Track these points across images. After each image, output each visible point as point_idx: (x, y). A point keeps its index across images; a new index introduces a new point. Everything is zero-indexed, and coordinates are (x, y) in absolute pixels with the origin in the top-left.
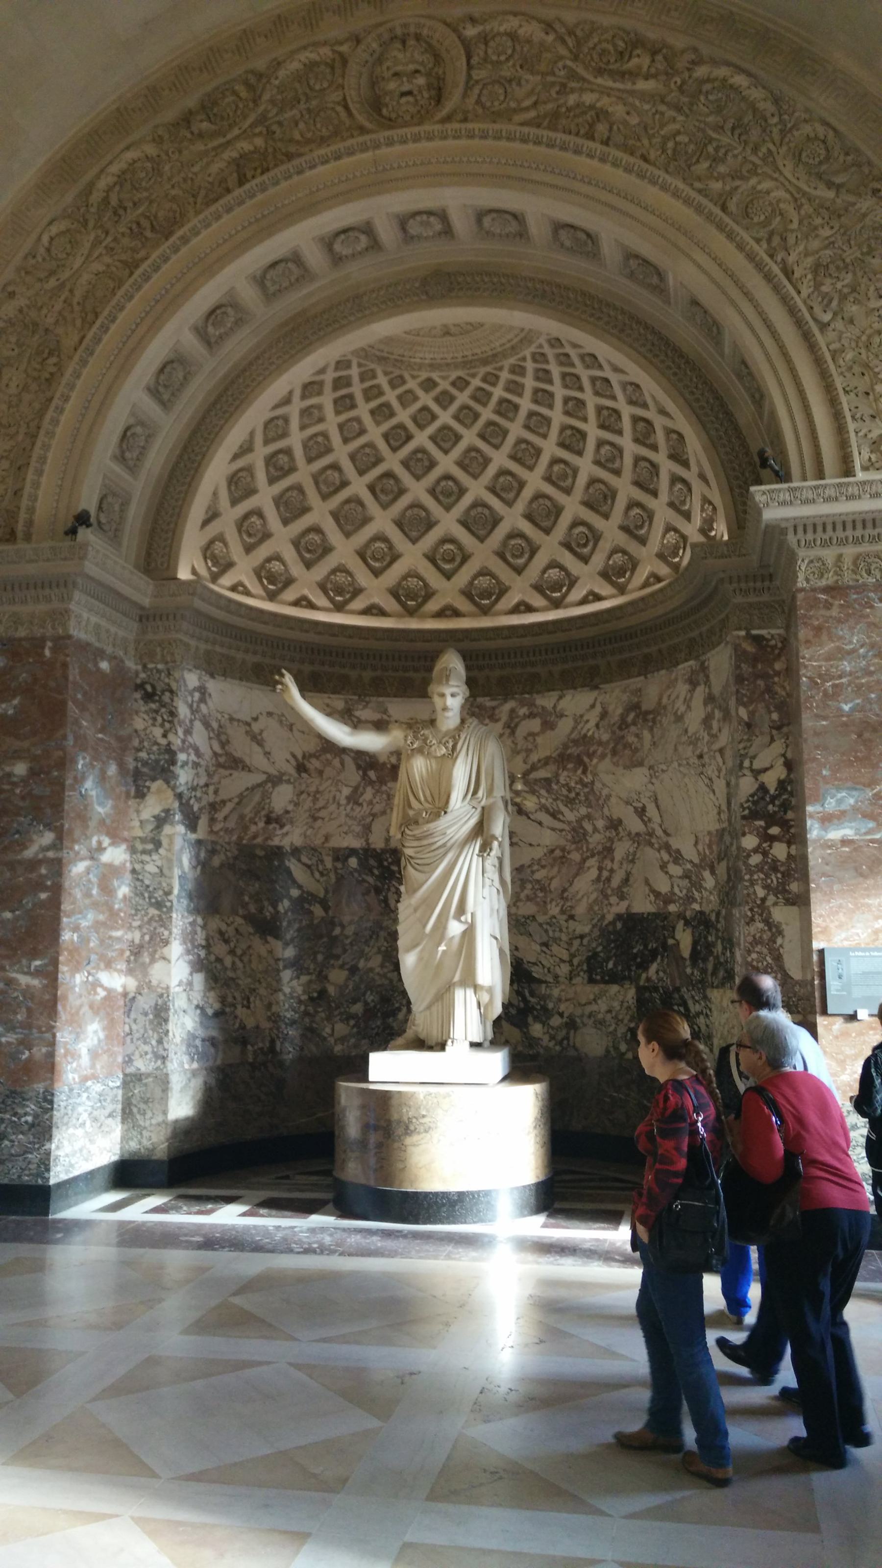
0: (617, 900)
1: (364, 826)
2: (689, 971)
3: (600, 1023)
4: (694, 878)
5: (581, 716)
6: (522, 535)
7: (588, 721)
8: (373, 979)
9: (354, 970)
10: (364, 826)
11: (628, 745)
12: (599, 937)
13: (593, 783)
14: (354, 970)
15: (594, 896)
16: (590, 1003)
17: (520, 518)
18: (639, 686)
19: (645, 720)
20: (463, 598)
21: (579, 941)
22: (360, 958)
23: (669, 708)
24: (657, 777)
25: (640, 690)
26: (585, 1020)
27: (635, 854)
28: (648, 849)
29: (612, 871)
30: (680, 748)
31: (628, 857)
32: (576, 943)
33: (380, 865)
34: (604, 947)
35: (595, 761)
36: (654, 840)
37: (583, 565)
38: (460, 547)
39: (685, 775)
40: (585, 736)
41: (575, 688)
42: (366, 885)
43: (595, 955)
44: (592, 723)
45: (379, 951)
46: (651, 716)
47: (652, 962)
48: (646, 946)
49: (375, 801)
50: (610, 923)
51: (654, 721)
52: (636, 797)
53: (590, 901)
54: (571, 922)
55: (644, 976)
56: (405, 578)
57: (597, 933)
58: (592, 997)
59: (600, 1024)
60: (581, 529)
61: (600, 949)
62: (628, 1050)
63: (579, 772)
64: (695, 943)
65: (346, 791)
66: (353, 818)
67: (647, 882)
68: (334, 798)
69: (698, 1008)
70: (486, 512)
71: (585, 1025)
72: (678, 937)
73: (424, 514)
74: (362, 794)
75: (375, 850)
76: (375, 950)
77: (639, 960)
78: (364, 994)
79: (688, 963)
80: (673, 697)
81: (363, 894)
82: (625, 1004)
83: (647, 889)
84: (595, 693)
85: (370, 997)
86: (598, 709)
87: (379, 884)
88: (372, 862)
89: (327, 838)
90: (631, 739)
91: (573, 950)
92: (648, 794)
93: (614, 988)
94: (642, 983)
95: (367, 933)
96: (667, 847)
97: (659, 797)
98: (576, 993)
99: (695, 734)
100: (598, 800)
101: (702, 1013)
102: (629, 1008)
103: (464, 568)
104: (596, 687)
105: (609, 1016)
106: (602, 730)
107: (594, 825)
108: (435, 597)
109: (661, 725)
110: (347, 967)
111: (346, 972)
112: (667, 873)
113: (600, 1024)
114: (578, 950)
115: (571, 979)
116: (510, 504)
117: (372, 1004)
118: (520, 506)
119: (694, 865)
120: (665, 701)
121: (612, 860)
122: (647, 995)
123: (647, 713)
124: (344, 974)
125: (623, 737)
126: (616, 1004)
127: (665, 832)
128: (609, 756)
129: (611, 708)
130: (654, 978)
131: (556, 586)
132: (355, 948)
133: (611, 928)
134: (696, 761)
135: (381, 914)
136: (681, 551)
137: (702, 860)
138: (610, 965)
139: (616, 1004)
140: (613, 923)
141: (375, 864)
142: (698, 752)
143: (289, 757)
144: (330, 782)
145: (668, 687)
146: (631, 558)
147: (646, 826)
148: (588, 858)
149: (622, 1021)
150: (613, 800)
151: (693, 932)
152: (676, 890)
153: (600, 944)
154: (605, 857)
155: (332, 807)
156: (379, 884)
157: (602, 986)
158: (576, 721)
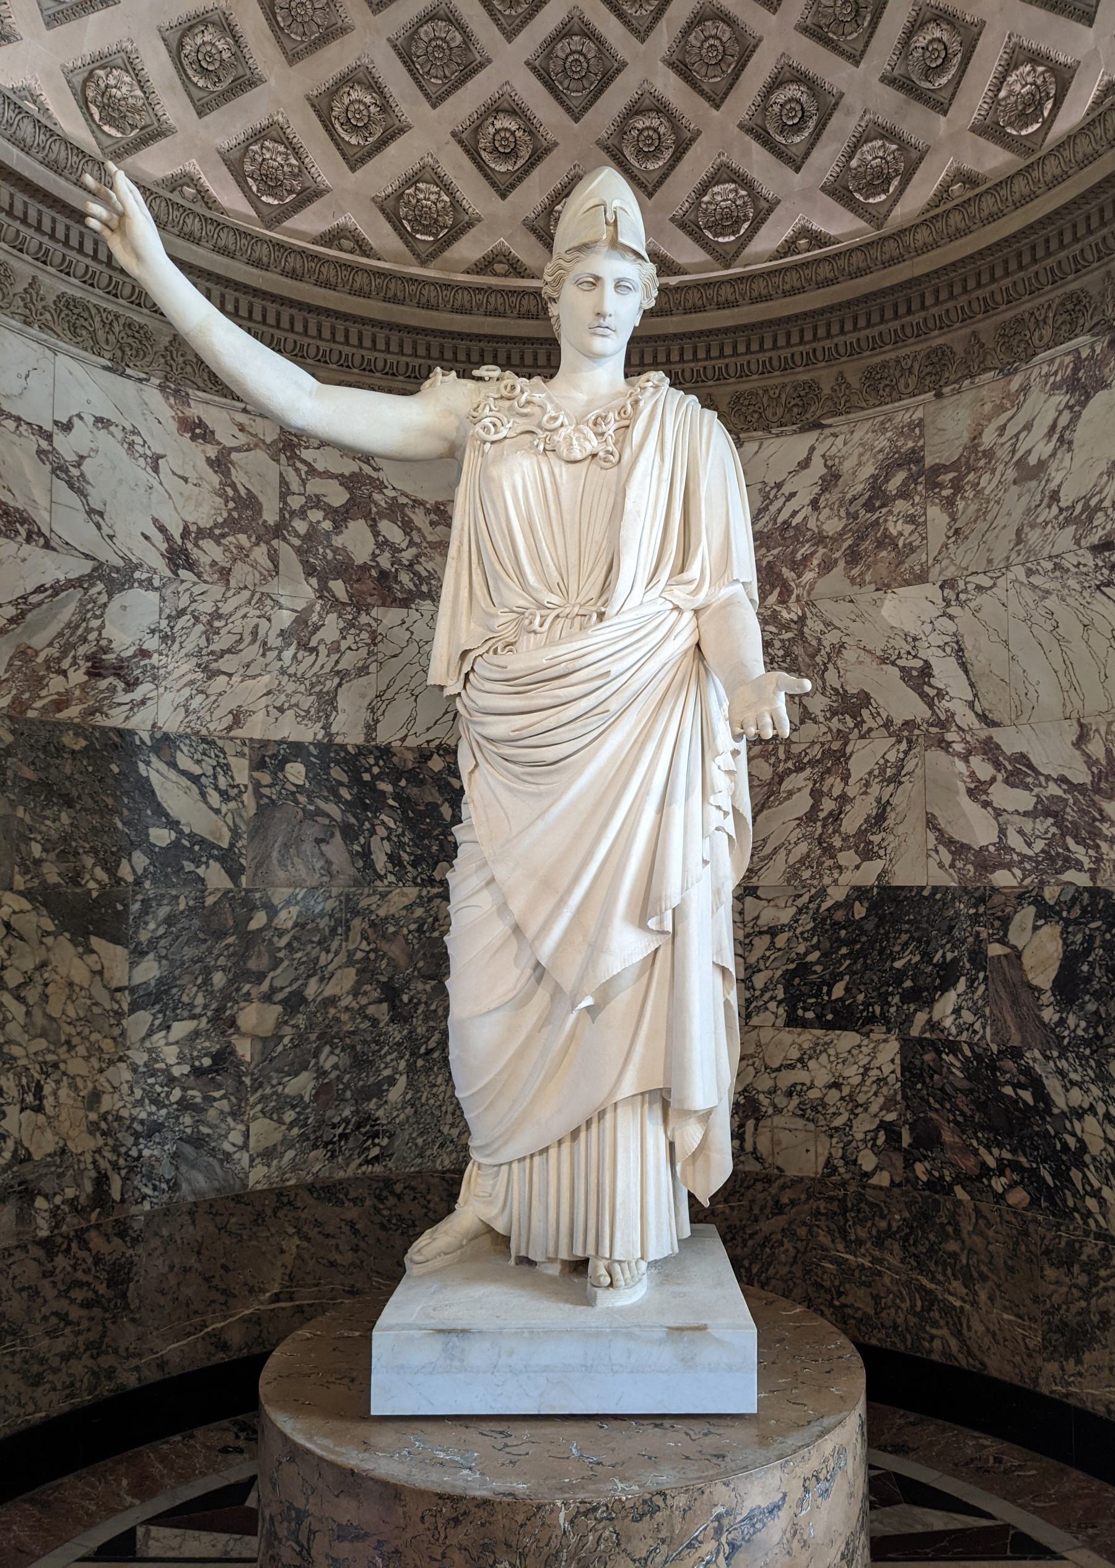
0: (858, 860)
1: (320, 695)
2: (1049, 1015)
3: (814, 1109)
4: (1071, 814)
5: (779, 486)
6: (661, 108)
7: (793, 495)
8: (337, 1020)
9: (294, 1002)
10: (320, 695)
11: (887, 541)
12: (814, 929)
13: (802, 619)
14: (294, 1002)
15: (803, 848)
16: (791, 1067)
17: (661, 64)
18: (919, 414)
19: (934, 485)
20: (533, 238)
21: (767, 938)
22: (309, 976)
23: (1002, 453)
24: (962, 604)
25: (921, 423)
26: (780, 1100)
27: (900, 765)
28: (936, 756)
29: (843, 799)
30: (1033, 536)
31: (883, 771)
32: (761, 944)
33: (356, 779)
34: (825, 955)
35: (809, 576)
36: (950, 736)
37: (789, 171)
38: (531, 129)
39: (1048, 592)
40: (786, 524)
41: (767, 429)
42: (327, 821)
43: (803, 968)
44: (804, 498)
45: (350, 962)
46: (951, 475)
47: (944, 988)
48: (927, 957)
49: (344, 645)
50: (837, 905)
51: (957, 486)
52: (909, 648)
53: (791, 861)
54: (749, 899)
55: (921, 1018)
56: (412, 180)
57: (806, 923)
58: (795, 1054)
59: (811, 1111)
60: (793, 91)
61: (814, 956)
62: (878, 1168)
63: (773, 598)
64: (1070, 961)
65: (285, 619)
66: (299, 679)
67: (931, 823)
68: (255, 633)
69: (1076, 1097)
70: (590, 49)
71: (778, 1111)
72: (1012, 938)
73: (459, 38)
74: (317, 628)
75: (343, 747)
76: (342, 958)
77: (908, 984)
78: (316, 1054)
79: (1047, 998)
80: (1011, 431)
81: (318, 841)
82: (874, 1073)
83: (932, 837)
84: (811, 437)
85: (328, 1059)
86: (817, 468)
87: (353, 820)
88: (337, 773)
89: (238, 717)
90: (895, 527)
91: (752, 959)
92: (937, 640)
93: (847, 1039)
94: (915, 1032)
95: (323, 923)
96: (990, 750)
97: (968, 643)
98: (759, 1045)
99: (1086, 499)
100: (813, 657)
101: (1092, 1109)
102: (881, 1081)
103: (536, 174)
104: (817, 425)
105: (833, 1096)
106: (826, 512)
107: (801, 703)
108: (473, 230)
109: (979, 493)
110: (280, 996)
111: (279, 1008)
112: (986, 804)
113: (811, 1111)
114: (764, 958)
115: (748, 1016)
116: (642, 34)
117: (334, 1075)
118: (664, 36)
119: (1080, 788)
120: (988, 438)
121: (845, 778)
122: (929, 1057)
123: (938, 469)
124: (275, 1011)
125: (876, 523)
126: (852, 1073)
127: (983, 718)
128: (842, 564)
129: (847, 466)
130: (948, 1022)
131: (727, 222)
132: (298, 955)
133: (839, 915)
134: (1089, 559)
135: (357, 883)
136: (1049, 105)
137: (1098, 778)
138: (838, 991)
139: (852, 1073)
140: (846, 905)
141: (344, 778)
142: (1095, 538)
143: (157, 537)
144: (246, 594)
145: (1000, 409)
146: (904, 146)
147: (931, 705)
148: (788, 772)
149: (866, 1106)
150: (849, 654)
151: (1064, 932)
152: (1015, 840)
153: (816, 947)
154: (828, 771)
155: (251, 652)
156: (353, 820)
157: (819, 1032)
158: (766, 497)
